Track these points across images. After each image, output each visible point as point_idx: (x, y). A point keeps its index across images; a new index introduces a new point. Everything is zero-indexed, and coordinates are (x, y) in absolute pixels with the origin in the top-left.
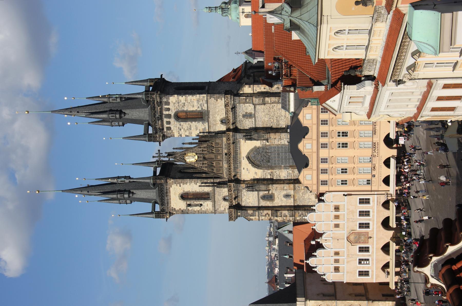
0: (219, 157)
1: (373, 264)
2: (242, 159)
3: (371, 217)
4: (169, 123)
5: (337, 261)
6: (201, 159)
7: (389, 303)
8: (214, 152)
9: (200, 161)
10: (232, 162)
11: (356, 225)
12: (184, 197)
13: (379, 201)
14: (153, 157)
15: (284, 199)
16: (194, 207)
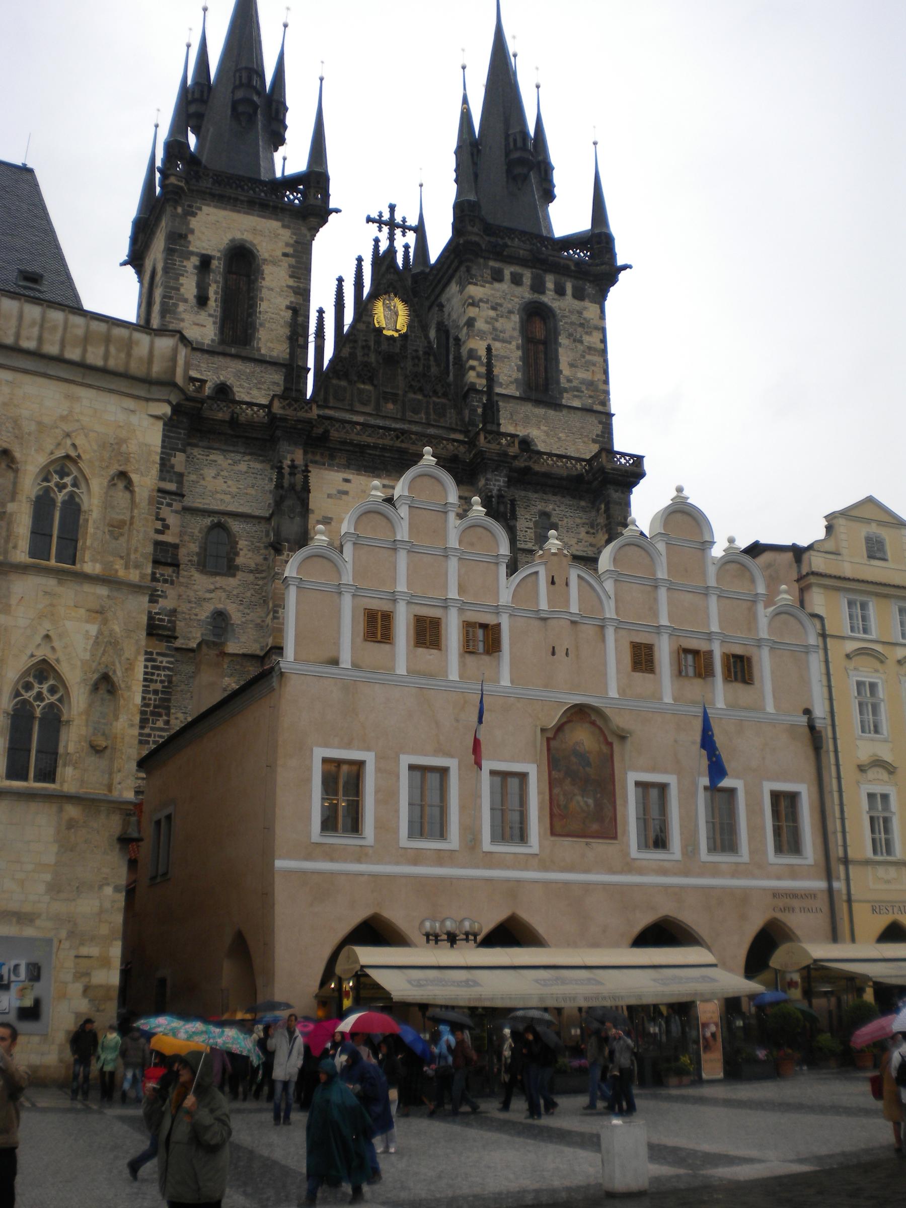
0: (390, 406)
1: (417, 858)
2: (386, 482)
3: (704, 855)
4: (516, 280)
5: (427, 633)
6: (384, 346)
7: (105, 962)
8: (411, 395)
9: (378, 343)
10: (387, 442)
11: (653, 769)
12: (242, 260)
13: (796, 903)
14: (392, 208)
15: (205, 613)
16: (195, 278)
